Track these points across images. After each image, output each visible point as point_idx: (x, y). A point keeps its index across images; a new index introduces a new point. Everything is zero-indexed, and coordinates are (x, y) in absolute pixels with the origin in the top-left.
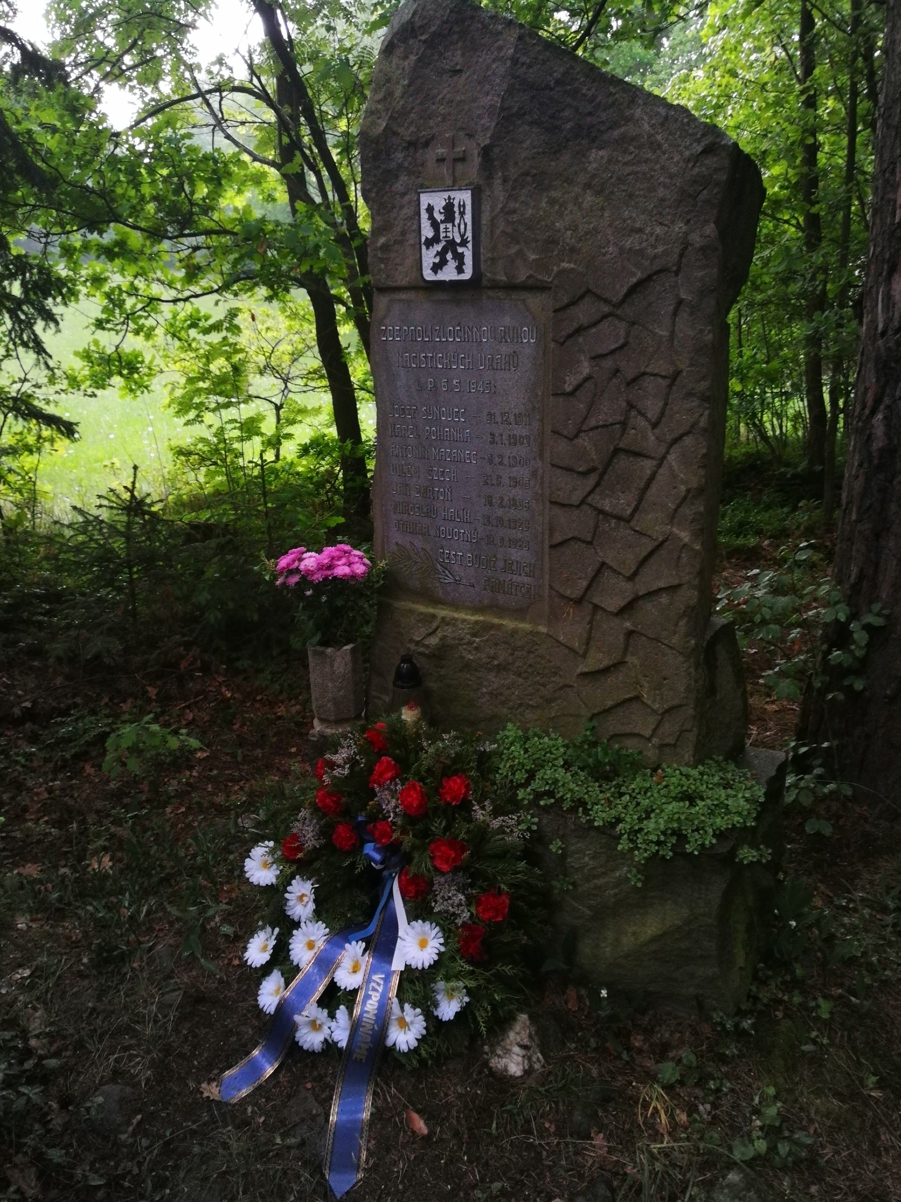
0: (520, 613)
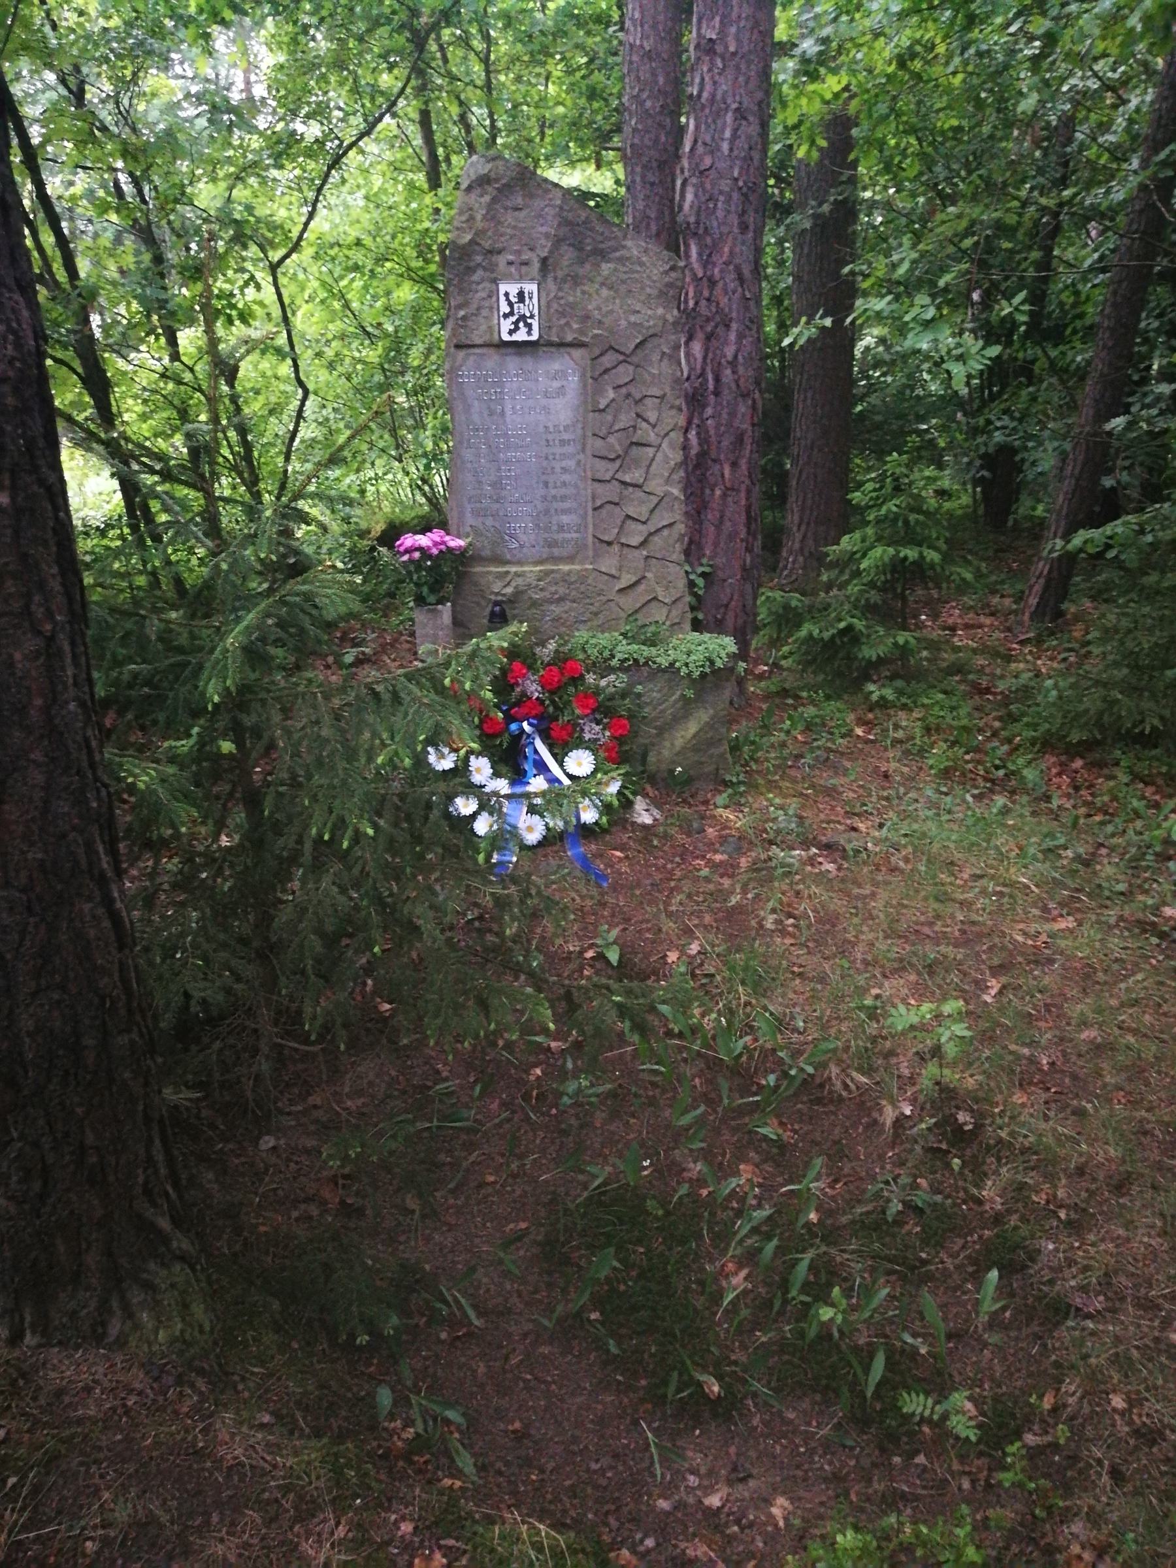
0: (571, 559)
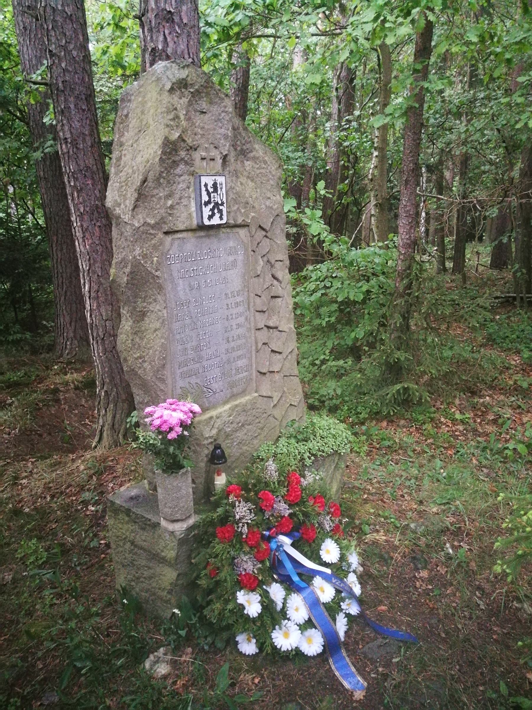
0: (243, 392)
